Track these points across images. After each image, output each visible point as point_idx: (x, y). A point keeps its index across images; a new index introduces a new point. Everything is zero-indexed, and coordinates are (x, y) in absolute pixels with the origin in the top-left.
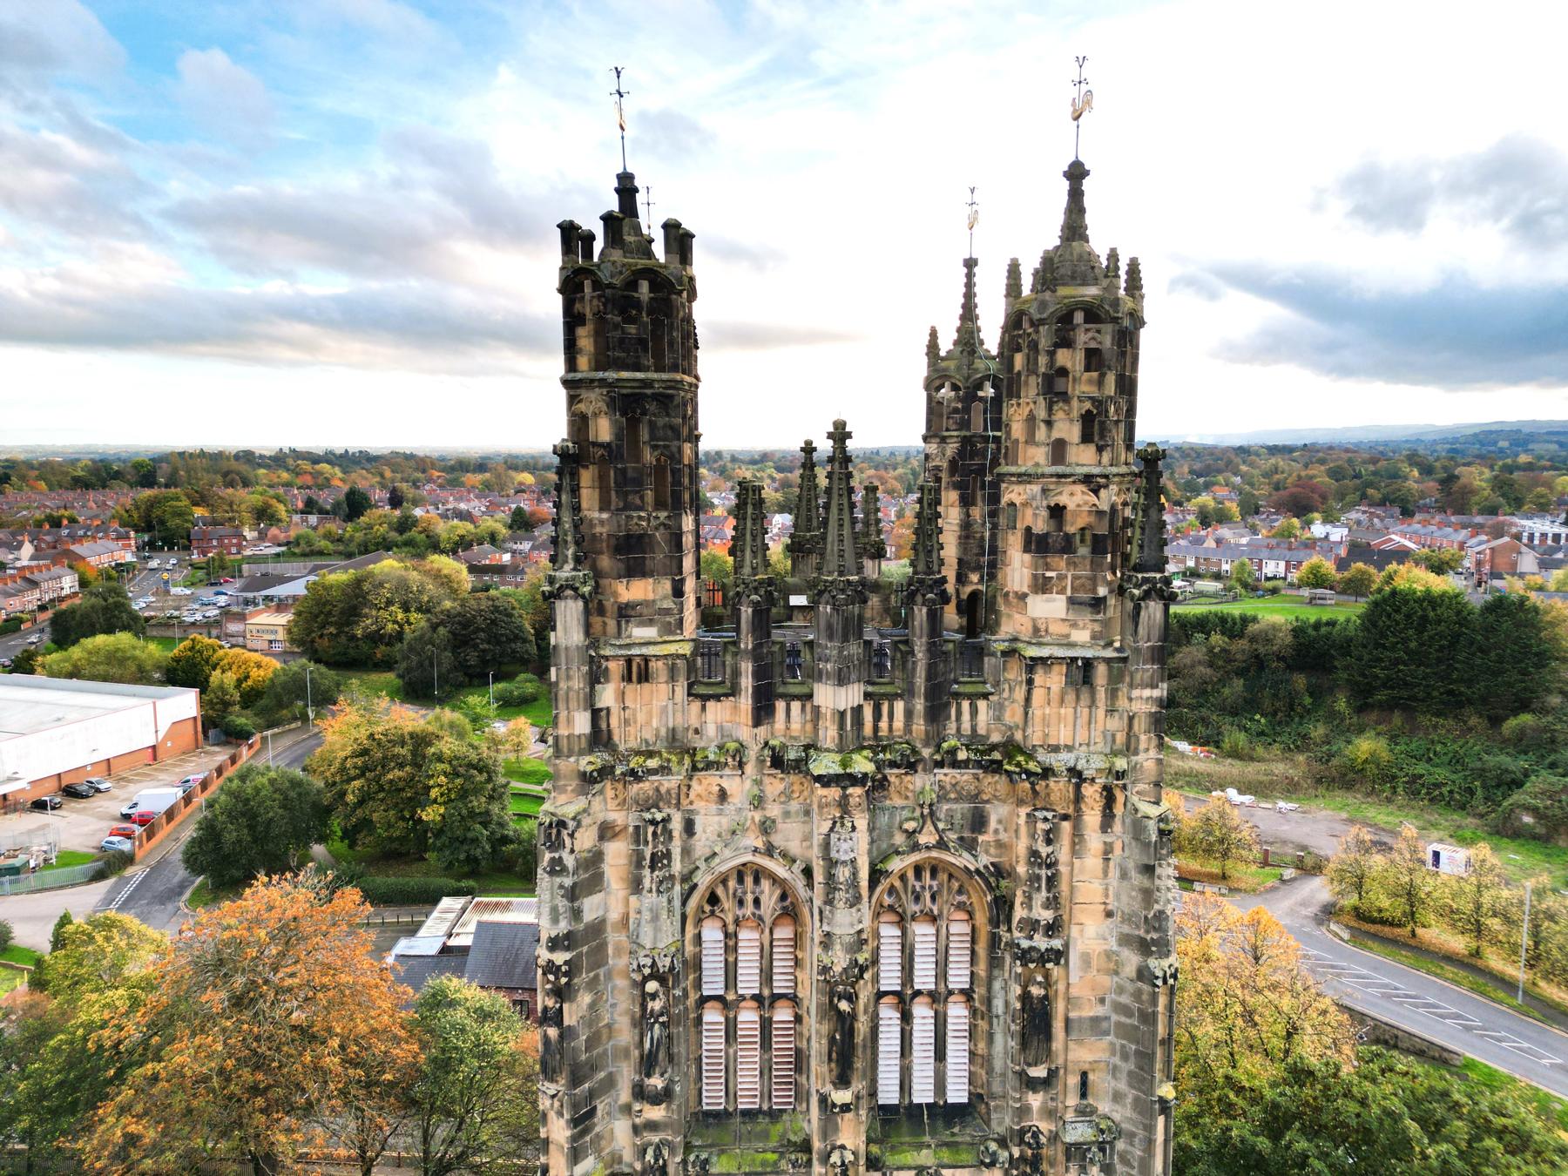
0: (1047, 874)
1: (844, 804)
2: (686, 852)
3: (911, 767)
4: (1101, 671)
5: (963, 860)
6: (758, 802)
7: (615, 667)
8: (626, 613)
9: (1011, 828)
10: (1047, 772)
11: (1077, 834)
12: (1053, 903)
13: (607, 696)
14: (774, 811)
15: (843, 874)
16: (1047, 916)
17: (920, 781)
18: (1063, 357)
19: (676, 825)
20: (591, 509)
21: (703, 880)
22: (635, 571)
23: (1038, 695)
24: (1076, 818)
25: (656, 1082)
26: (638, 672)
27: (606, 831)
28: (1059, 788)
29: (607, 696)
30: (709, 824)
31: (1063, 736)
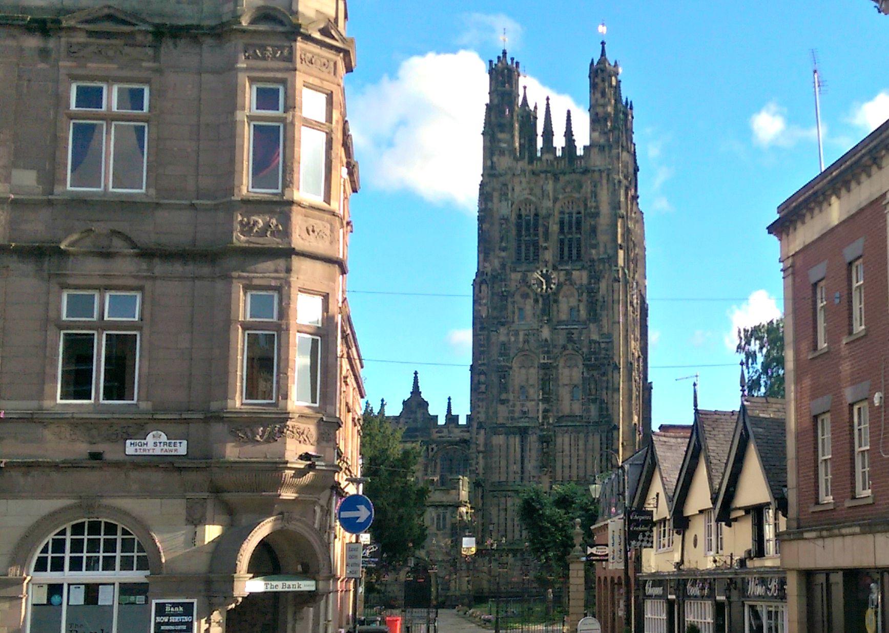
0: (595, 194)
1: (546, 179)
2: (512, 195)
3: (565, 174)
4: (606, 149)
5: (577, 195)
6: (529, 183)
7: (497, 153)
8: (500, 141)
9: (587, 188)
10: (594, 171)
11: (601, 185)
12: (596, 201)
13: (495, 159)
14: (532, 185)
15: (546, 193)
16: (594, 204)
17: (567, 177)
18: (596, 80)
19: (510, 187)
20: (493, 118)
21: (516, 202)
22: (502, 131)
23: (592, 153)
24: (600, 182)
25: (504, 244)
26: (502, 153)
27: (494, 190)
28: (596, 175)
29: (495, 159)
30: (517, 189)
31: (598, 163)
